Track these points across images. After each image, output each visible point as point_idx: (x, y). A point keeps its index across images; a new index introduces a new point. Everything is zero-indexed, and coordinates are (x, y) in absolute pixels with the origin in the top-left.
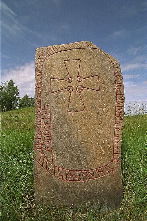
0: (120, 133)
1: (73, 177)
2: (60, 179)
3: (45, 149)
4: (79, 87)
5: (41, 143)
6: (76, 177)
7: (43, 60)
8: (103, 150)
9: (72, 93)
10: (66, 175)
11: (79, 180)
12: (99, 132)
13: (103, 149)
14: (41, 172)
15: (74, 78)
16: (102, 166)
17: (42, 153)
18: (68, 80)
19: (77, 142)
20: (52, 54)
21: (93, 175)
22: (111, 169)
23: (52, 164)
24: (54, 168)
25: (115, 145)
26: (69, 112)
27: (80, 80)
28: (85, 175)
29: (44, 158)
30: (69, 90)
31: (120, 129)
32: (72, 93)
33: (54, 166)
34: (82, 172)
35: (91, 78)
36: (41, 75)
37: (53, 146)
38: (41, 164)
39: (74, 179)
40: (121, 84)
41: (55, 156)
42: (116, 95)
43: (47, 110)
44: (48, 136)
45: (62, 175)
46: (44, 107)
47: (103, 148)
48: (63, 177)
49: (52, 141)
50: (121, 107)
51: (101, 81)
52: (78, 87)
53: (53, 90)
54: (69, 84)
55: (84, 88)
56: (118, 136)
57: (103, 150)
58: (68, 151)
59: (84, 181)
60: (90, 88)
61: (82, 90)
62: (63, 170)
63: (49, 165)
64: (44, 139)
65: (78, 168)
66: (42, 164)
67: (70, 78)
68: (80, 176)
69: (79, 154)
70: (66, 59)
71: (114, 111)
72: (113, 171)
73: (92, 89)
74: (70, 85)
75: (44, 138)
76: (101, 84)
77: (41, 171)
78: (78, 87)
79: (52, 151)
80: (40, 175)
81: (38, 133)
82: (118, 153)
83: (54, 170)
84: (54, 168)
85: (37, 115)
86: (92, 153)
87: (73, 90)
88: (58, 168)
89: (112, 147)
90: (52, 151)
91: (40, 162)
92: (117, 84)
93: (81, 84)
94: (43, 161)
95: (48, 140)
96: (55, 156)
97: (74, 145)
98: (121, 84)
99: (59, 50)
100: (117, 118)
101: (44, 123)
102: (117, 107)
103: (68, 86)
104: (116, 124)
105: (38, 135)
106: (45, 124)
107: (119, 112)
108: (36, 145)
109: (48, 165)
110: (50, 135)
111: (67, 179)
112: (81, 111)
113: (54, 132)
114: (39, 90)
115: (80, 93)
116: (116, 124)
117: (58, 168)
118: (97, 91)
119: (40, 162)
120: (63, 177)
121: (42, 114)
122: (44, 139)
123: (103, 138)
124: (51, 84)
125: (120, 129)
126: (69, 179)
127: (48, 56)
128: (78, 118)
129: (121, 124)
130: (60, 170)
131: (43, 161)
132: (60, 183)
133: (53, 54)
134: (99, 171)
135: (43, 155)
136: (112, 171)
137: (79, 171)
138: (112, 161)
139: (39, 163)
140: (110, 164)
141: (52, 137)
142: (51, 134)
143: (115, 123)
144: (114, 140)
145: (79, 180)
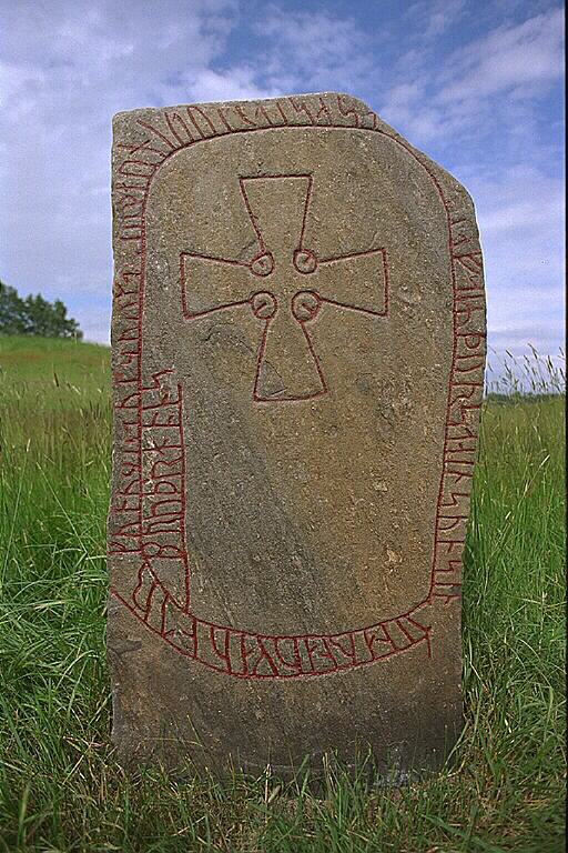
0: (462, 491)
1: (271, 663)
2: (219, 670)
3: (159, 554)
4: (301, 297)
5: (140, 528)
6: (282, 661)
7: (147, 169)
8: (392, 557)
10: (244, 655)
11: (296, 671)
14: (139, 645)
15: (283, 256)
16: (385, 618)
17: (143, 566)
18: (256, 265)
19: (288, 522)
20: (187, 145)
21: (351, 653)
22: (423, 629)
23: (186, 611)
24: (194, 628)
26: (259, 400)
27: (307, 267)
28: (320, 654)
29: (153, 589)
31: (463, 475)
33: (195, 620)
34: (306, 641)
35: (355, 258)
36: (138, 238)
37: (192, 540)
38: (138, 611)
39: (275, 670)
40: (474, 292)
41: (200, 581)
43: (167, 388)
44: (171, 497)
45: (227, 652)
48: (229, 665)
49: (187, 520)
50: (470, 387)
51: (396, 276)
53: (192, 308)
54: (260, 283)
55: (325, 303)
56: (455, 502)
57: (392, 557)
58: (253, 562)
59: (313, 678)
61: (313, 311)
62: (232, 634)
63: (175, 618)
64: (153, 512)
65: (290, 625)
66: (142, 615)
67: (266, 254)
68: (299, 659)
69: (298, 573)
70: (248, 172)
71: (442, 400)
72: (431, 639)
73: (357, 308)
74: (267, 287)
75: (154, 507)
77: (140, 639)
79: (186, 562)
80: (137, 655)
81: (128, 489)
82: (451, 569)
83: (193, 636)
84: (194, 628)
85: (123, 412)
86: (349, 568)
87: (279, 310)
88: (212, 630)
90: (186, 562)
91: (133, 605)
93: (311, 286)
94: (149, 600)
96: (200, 581)
97: (278, 534)
98: (474, 292)
99: (220, 127)
100: (454, 430)
102: (456, 384)
103: (256, 289)
104: (448, 456)
105: (126, 492)
106: (157, 448)
107: (463, 407)
108: (118, 537)
109: (168, 616)
110: (178, 496)
111: (246, 670)
112: (308, 397)
113: (196, 483)
115: (306, 325)
116: (448, 456)
117: (212, 630)
118: (377, 317)
119: (133, 605)
120: (229, 665)
121: (144, 409)
122: (153, 512)
124: (182, 281)
125: (463, 475)
126: (255, 670)
127: (171, 153)
128: (294, 427)
129: (465, 456)
130: (220, 634)
131: (149, 600)
132: (218, 687)
133: (193, 141)
134: (374, 637)
135: (148, 576)
136: (426, 637)
137: (294, 638)
138: (427, 600)
139: (132, 610)
140: (418, 610)
143: (445, 452)
144: (438, 517)
145: (296, 671)
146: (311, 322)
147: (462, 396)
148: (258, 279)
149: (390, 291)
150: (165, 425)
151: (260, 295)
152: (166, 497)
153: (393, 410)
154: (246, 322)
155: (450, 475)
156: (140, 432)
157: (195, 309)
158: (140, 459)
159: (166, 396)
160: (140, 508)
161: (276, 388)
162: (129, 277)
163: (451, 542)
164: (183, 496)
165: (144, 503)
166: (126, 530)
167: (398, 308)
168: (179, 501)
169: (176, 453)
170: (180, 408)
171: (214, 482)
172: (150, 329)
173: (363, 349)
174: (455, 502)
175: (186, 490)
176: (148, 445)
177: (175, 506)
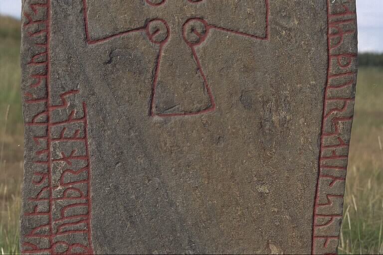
4: (191, 23)
5: (51, 229)
9: (166, 45)
12: (261, 189)
13: (275, 248)
25: (316, 232)
30: (155, 32)
31: (336, 178)
32: (167, 43)
40: (346, 17)
42: (325, 58)
44: (78, 201)
46: (61, 96)
47: (275, 243)
50: (342, 101)
52: (187, 22)
54: (154, 11)
56: (329, 202)
60: (229, 26)
64: (62, 214)
71: (317, 113)
73: (242, 33)
74: (160, 15)
76: (272, 14)
78: (187, 22)
85: (34, 127)
87: (170, 37)
89: (307, 239)
92: (334, 14)
93: (199, 14)
95: (79, 218)
98: (346, 17)
101: (61, 155)
102: (330, 99)
105: (37, 198)
107: (335, 120)
112: (199, 111)
114: (37, 31)
115: (196, 48)
118: (259, 40)
121: (54, 124)
122: (62, 214)
123: (276, 210)
124: (83, 10)
125: (336, 178)
141: (93, 205)
142: (88, 195)
146: (201, 46)
147: (334, 110)
148: (152, 8)
149: (270, 17)
150: (73, 138)
151: (154, 22)
152: (74, 201)
153: (273, 122)
154: (142, 46)
155: (325, 178)
156: (48, 145)
157: (97, 36)
158: (49, 168)
159: (73, 112)
160: (49, 211)
161: (169, 105)
162: (37, 7)
163: (327, 237)
164: (88, 200)
165: (53, 207)
166: (38, 231)
167: (278, 33)
168: (85, 204)
169: (83, 163)
170: (85, 123)
171: (116, 188)
172: (57, 53)
173: (247, 69)
174: (329, 202)
175: (92, 194)
176: (58, 156)
177: (80, 209)
